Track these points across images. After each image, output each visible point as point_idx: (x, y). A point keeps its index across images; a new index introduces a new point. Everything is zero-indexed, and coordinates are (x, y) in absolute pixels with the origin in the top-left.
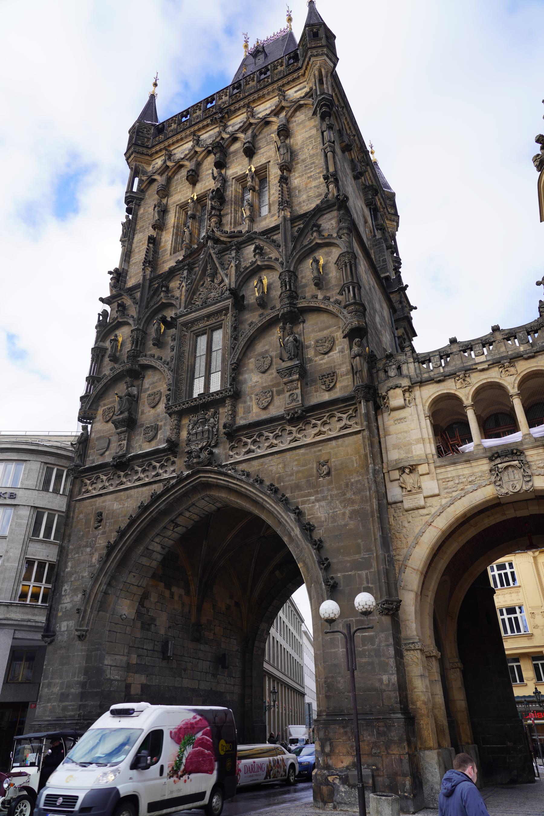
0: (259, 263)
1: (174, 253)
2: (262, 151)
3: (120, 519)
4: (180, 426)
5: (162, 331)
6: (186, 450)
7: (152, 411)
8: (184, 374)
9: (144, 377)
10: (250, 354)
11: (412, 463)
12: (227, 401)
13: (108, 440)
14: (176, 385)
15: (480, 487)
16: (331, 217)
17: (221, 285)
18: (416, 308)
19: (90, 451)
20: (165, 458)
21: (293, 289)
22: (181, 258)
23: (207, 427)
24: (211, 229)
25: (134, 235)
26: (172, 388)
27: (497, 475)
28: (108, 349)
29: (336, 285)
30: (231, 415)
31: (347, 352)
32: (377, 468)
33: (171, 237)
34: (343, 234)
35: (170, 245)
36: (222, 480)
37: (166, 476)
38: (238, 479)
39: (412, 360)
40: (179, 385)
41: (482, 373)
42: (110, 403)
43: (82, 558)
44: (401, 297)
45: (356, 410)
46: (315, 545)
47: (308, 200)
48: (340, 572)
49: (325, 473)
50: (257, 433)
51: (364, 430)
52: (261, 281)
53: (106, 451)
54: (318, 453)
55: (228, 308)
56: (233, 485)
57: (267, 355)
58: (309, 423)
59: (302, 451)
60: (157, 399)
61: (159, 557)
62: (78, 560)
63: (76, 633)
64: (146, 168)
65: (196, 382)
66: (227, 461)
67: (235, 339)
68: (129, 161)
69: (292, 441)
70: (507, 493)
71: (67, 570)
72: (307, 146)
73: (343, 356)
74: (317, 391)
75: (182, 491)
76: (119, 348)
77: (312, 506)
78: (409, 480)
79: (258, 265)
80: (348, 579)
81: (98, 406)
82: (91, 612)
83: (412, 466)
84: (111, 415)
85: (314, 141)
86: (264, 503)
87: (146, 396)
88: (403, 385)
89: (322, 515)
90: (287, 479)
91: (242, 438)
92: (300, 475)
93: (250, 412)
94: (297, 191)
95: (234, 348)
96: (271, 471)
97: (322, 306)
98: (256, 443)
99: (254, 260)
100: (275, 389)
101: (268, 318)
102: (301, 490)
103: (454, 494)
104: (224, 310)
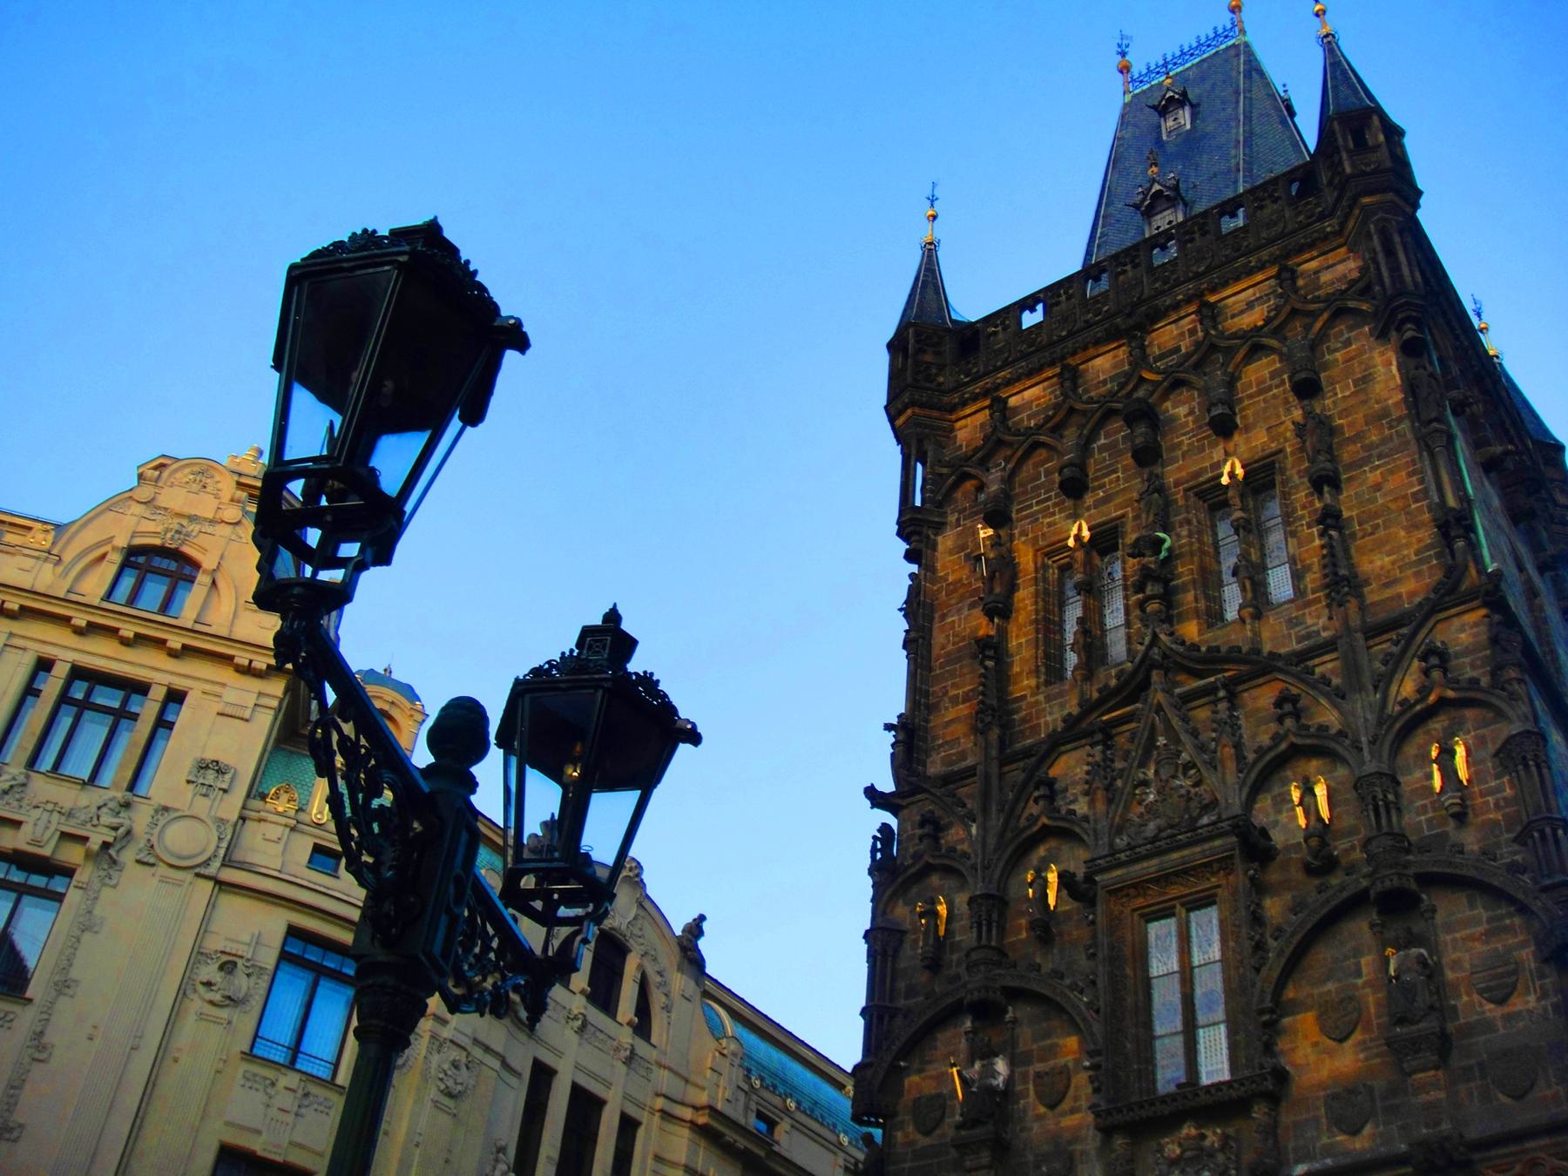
5: (1052, 901)
67: (1259, 947)
68: (899, 422)
95: (1258, 970)
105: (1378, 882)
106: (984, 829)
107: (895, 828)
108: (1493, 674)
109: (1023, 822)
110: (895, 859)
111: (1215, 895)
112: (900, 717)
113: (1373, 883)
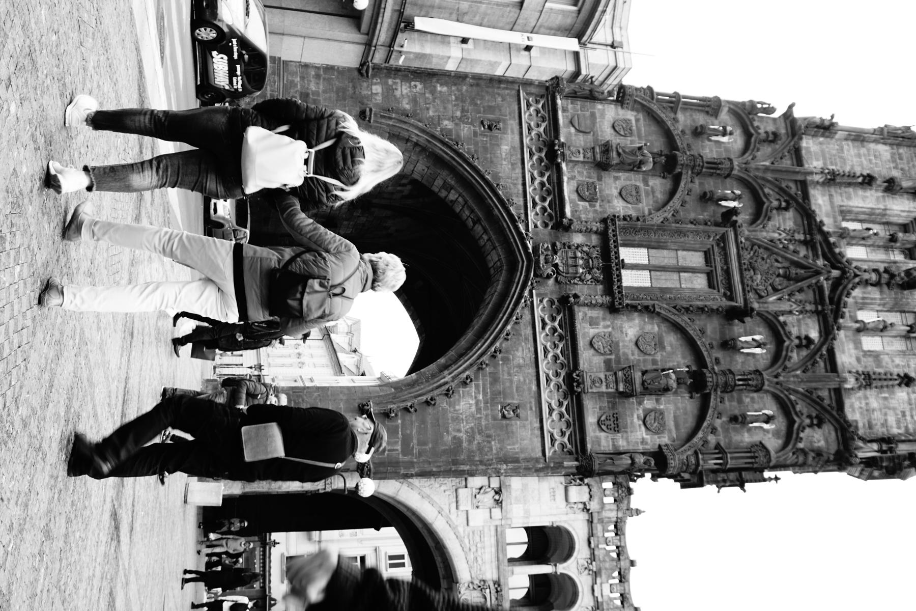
0: (787, 343)
1: (842, 212)
3: (489, 156)
4: (590, 232)
5: (723, 203)
6: (557, 243)
7: (615, 192)
8: (656, 237)
9: (664, 177)
10: (664, 327)
11: (503, 503)
12: (608, 298)
13: (588, 131)
14: (642, 229)
15: (470, 567)
16: (830, 440)
17: (770, 288)
18: (719, 492)
19: (579, 103)
20: (553, 214)
21: (737, 388)
22: (825, 229)
23: (581, 270)
24: (858, 273)
25: (891, 145)
26: (639, 223)
27: (479, 587)
28: (716, 117)
29: (730, 441)
30: (591, 303)
31: (641, 448)
32: (502, 471)
33: (871, 205)
34: (797, 458)
36: (515, 290)
37: (531, 215)
38: (513, 310)
39: (620, 515)
40: (643, 232)
41: (590, 588)
42: (638, 129)
43: (450, 106)
44: (731, 481)
45: (570, 453)
46: (432, 399)
47: (867, 410)
48: (402, 423)
49: (506, 412)
50: (563, 334)
52: (759, 345)
53: (576, 128)
54: (528, 405)
55: (731, 298)
56: (508, 302)
57: (658, 349)
58: (565, 398)
59: (534, 388)
60: (630, 199)
61: (443, 194)
62: (448, 101)
63: (368, 109)
65: (644, 251)
66: (537, 295)
67: (687, 310)
69: (547, 376)
70: (460, 592)
71: (438, 85)
73: (637, 443)
74: (600, 409)
75: (511, 237)
76: (714, 138)
77: (472, 396)
78: (488, 498)
79: (784, 341)
81: (638, 111)
82: (388, 125)
83: (501, 502)
84: (622, 133)
86: (483, 341)
87: (638, 184)
88: (592, 503)
89: (461, 407)
90: (506, 369)
91: (561, 315)
92: (508, 384)
93: (590, 325)
94: (887, 395)
95: (674, 307)
96: (517, 350)
97: (705, 424)
98: (552, 331)
99: (793, 337)
100: (613, 357)
101: (705, 354)
102: (491, 384)
103: (466, 541)
105: (710, 375)
106: (767, 169)
107: (776, 115)
108: (802, 450)
109: (767, 190)
110: (756, 114)
111: (714, 288)
112: (837, 123)
113: (710, 373)
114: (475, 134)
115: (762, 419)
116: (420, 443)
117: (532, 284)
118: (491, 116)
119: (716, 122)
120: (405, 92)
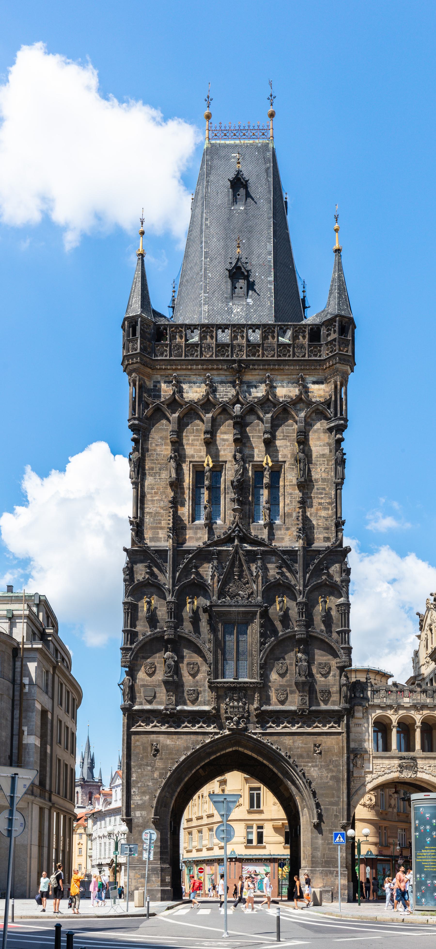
2: (278, 443)
23: (240, 704)
31: (338, 678)
35: (187, 510)
43: (145, 773)
49: (318, 751)
51: (343, 733)
60: (196, 669)
62: (141, 774)
64: (148, 383)
66: (255, 729)
67: (262, 644)
72: (320, 464)
73: (335, 680)
80: (327, 809)
84: (153, 669)
85: (326, 462)
90: (295, 750)
92: (303, 749)
95: (261, 651)
96: (285, 743)
97: (327, 640)
102: (303, 758)
104: (252, 613)
114: (161, 759)
115: (324, 606)
116: (333, 797)
117: (250, 733)
118: (149, 749)
119: (140, 604)
120: (138, 798)
